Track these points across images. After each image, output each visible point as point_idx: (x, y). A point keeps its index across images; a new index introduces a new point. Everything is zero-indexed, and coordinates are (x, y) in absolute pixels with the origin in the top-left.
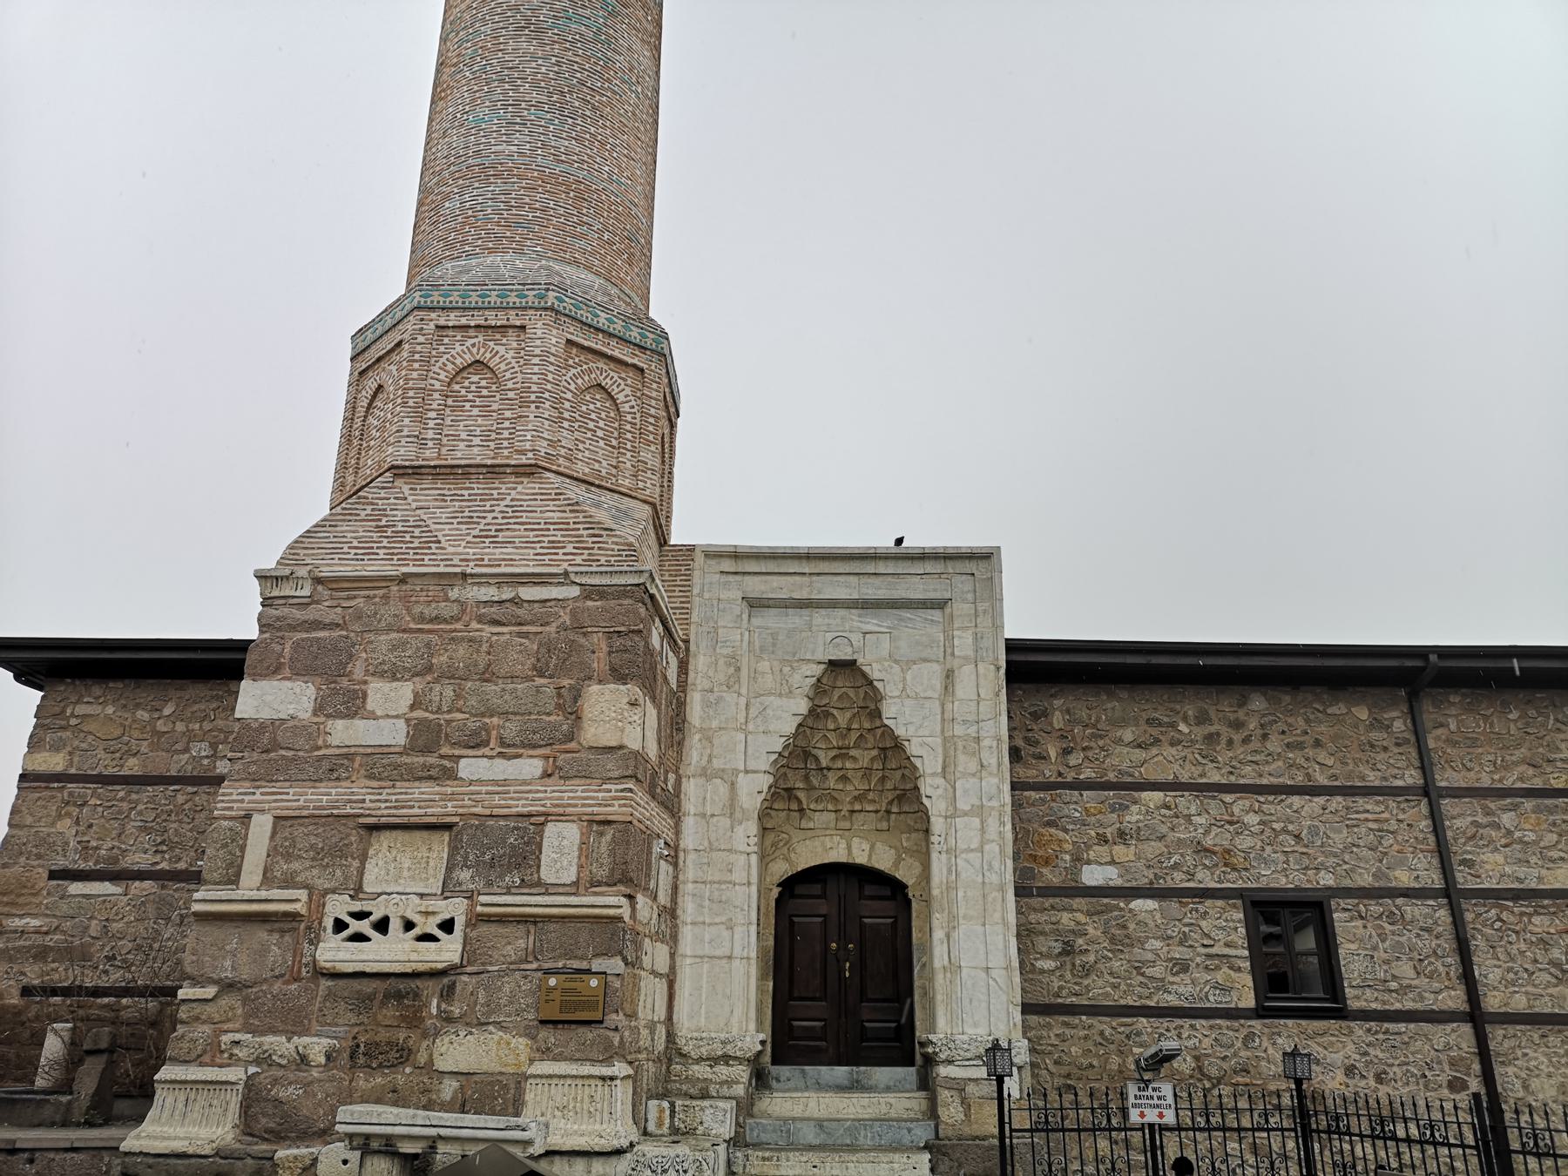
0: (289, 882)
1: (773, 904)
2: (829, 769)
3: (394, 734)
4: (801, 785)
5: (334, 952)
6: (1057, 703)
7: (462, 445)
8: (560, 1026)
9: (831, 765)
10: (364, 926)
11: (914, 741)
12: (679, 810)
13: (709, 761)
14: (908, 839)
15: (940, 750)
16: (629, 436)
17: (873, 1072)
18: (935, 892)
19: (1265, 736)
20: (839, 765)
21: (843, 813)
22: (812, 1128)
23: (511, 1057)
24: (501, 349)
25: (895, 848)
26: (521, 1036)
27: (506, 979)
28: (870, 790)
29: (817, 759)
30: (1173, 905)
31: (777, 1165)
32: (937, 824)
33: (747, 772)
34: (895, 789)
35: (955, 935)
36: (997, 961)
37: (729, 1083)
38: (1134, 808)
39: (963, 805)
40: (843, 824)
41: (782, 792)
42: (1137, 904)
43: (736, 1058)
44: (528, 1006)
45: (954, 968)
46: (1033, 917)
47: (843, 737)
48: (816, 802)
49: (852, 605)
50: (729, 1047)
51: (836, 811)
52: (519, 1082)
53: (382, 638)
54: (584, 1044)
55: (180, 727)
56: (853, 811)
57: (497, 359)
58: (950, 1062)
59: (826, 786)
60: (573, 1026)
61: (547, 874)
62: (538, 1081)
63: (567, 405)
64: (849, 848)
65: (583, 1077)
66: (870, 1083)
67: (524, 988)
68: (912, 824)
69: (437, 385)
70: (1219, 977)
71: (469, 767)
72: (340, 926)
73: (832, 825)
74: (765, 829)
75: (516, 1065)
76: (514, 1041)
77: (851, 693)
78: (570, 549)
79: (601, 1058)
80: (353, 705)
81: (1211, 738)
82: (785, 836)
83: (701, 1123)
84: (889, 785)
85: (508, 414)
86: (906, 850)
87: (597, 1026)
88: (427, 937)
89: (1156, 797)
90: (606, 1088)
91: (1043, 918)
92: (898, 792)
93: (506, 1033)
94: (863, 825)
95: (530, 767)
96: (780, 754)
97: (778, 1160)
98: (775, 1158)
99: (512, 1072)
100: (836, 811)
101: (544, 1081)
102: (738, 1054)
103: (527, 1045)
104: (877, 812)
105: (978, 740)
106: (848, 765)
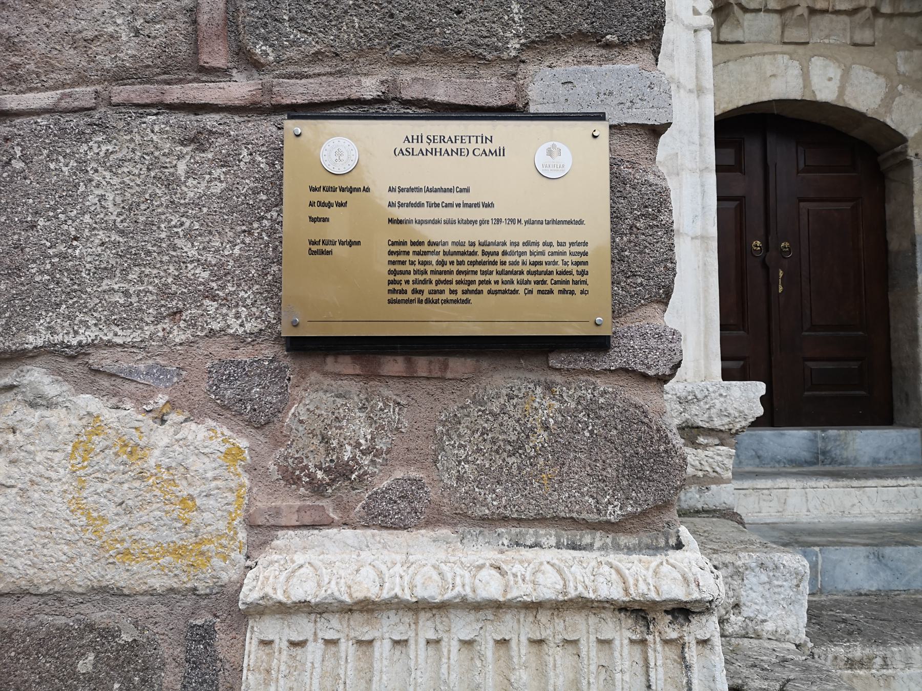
8: (394, 365)
17: (850, 438)
21: (799, 11)
22: (862, 560)
23: (154, 512)
25: (887, 76)
26: (195, 414)
27: (98, 146)
31: (887, 678)
40: (795, 34)
43: (711, 432)
44: (220, 273)
50: (694, 409)
51: (780, 12)
52: (205, 635)
54: (517, 448)
60: (459, 366)
62: (302, 628)
64: (805, 75)
65: (533, 607)
66: (845, 454)
67: (192, 189)
73: (775, 35)
75: (178, 551)
76: (162, 436)
79: (613, 513)
83: (737, 606)
86: (906, 80)
87: (581, 361)
90: (659, 656)
93: (116, 398)
94: (828, 37)
97: (885, 665)
98: (879, 661)
99: (158, 583)
100: (780, 12)
101: (332, 628)
102: (717, 423)
103: (233, 455)
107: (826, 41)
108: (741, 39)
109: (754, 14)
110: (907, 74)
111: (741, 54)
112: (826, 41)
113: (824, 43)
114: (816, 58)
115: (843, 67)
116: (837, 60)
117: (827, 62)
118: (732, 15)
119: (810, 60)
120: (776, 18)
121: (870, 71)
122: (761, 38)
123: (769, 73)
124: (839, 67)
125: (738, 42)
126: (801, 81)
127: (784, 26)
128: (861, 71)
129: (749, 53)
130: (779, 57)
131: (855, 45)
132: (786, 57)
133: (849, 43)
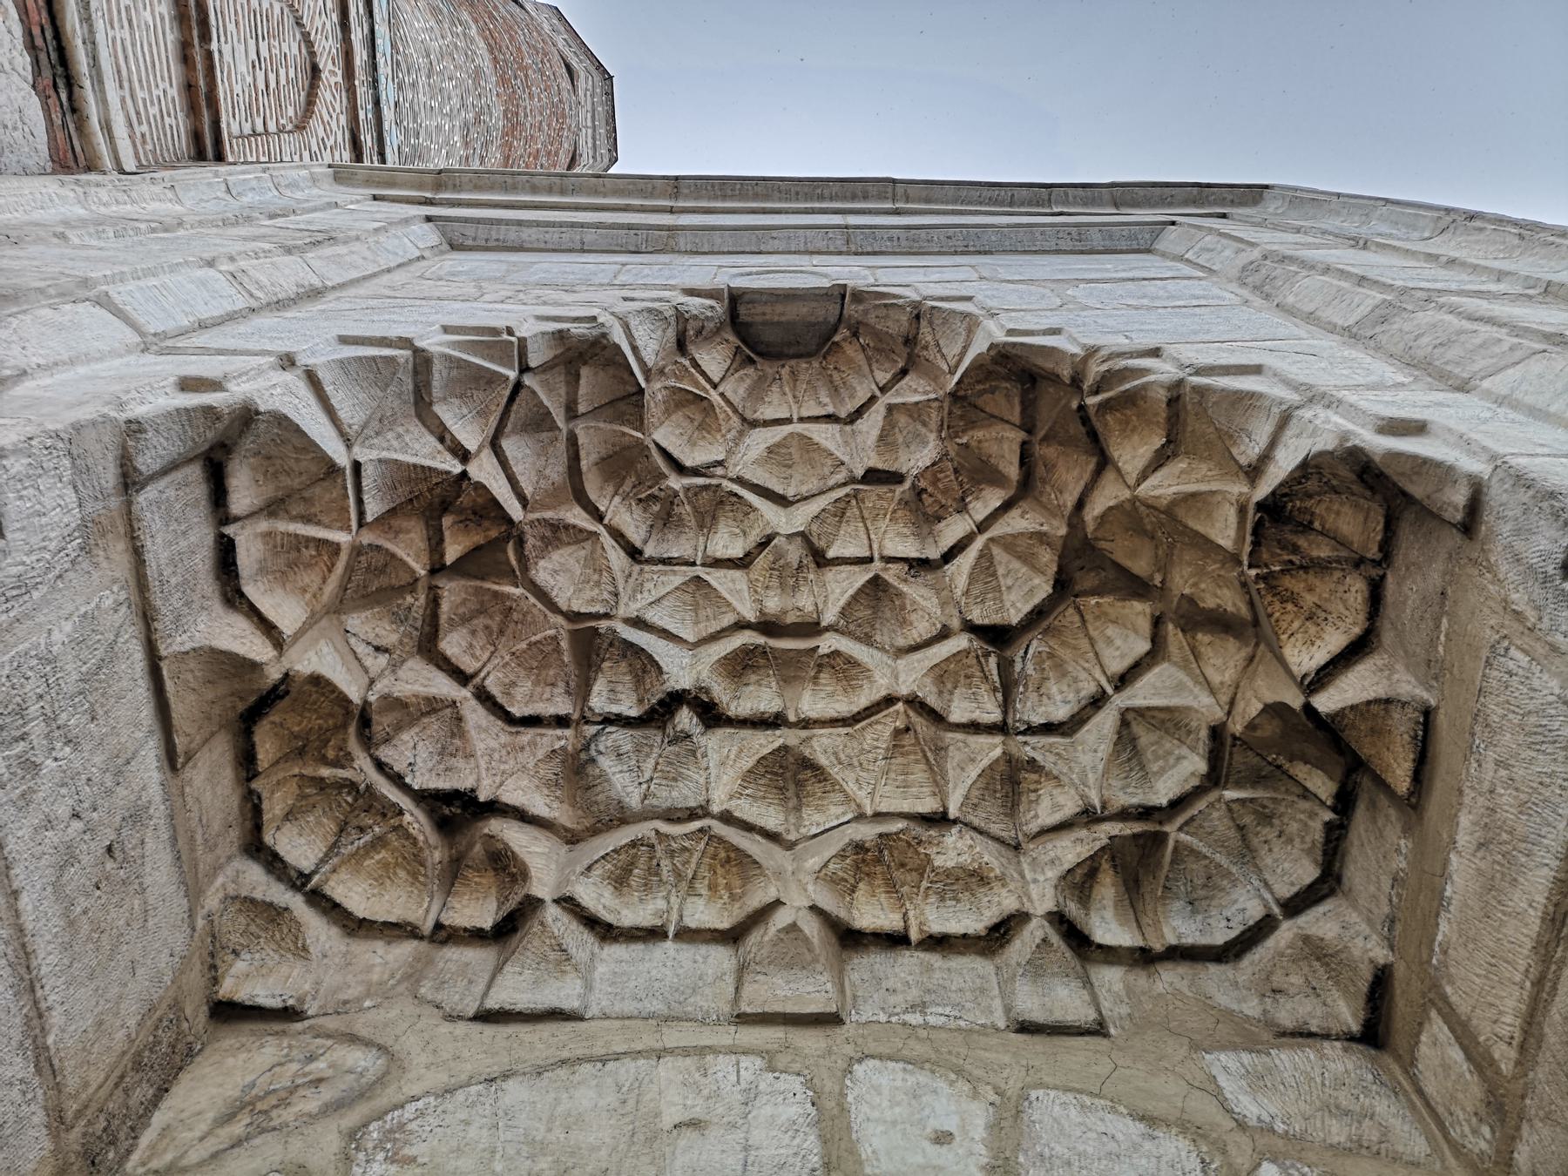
2: (711, 715)
4: (539, 805)
9: (721, 692)
14: (1257, 1081)
20: (760, 697)
21: (781, 919)
25: (1187, 1127)
28: (939, 820)
29: (643, 665)
34: (1089, 816)
41: (416, 820)
47: (789, 578)
48: (620, 881)
49: (821, 245)
51: (732, 936)
56: (849, 938)
59: (684, 795)
68: (1252, 1008)
74: (228, 1012)
77: (824, 434)
82: (360, 1059)
84: (1050, 806)
92: (1115, 828)
96: (422, 362)
100: (732, 936)
104: (1001, 933)
106: (813, 702)
107: (915, 1019)
108: (570, 1003)
109: (638, 948)
110: (1280, 1127)
111: (565, 1054)
112: (915, 1019)
113: (904, 1024)
114: (871, 1063)
115: (993, 1097)
116: (959, 1072)
117: (923, 1077)
118: (536, 928)
119: (848, 1071)
120: (720, 958)
121: (1113, 1110)
122: (657, 1006)
123: (671, 1116)
124: (975, 1095)
125: (555, 1015)
126: (811, 1142)
127: (741, 970)
128: (1073, 1112)
129: (599, 1050)
130: (723, 1064)
131: (1026, 1028)
132: (751, 1064)
133: (1002, 1024)
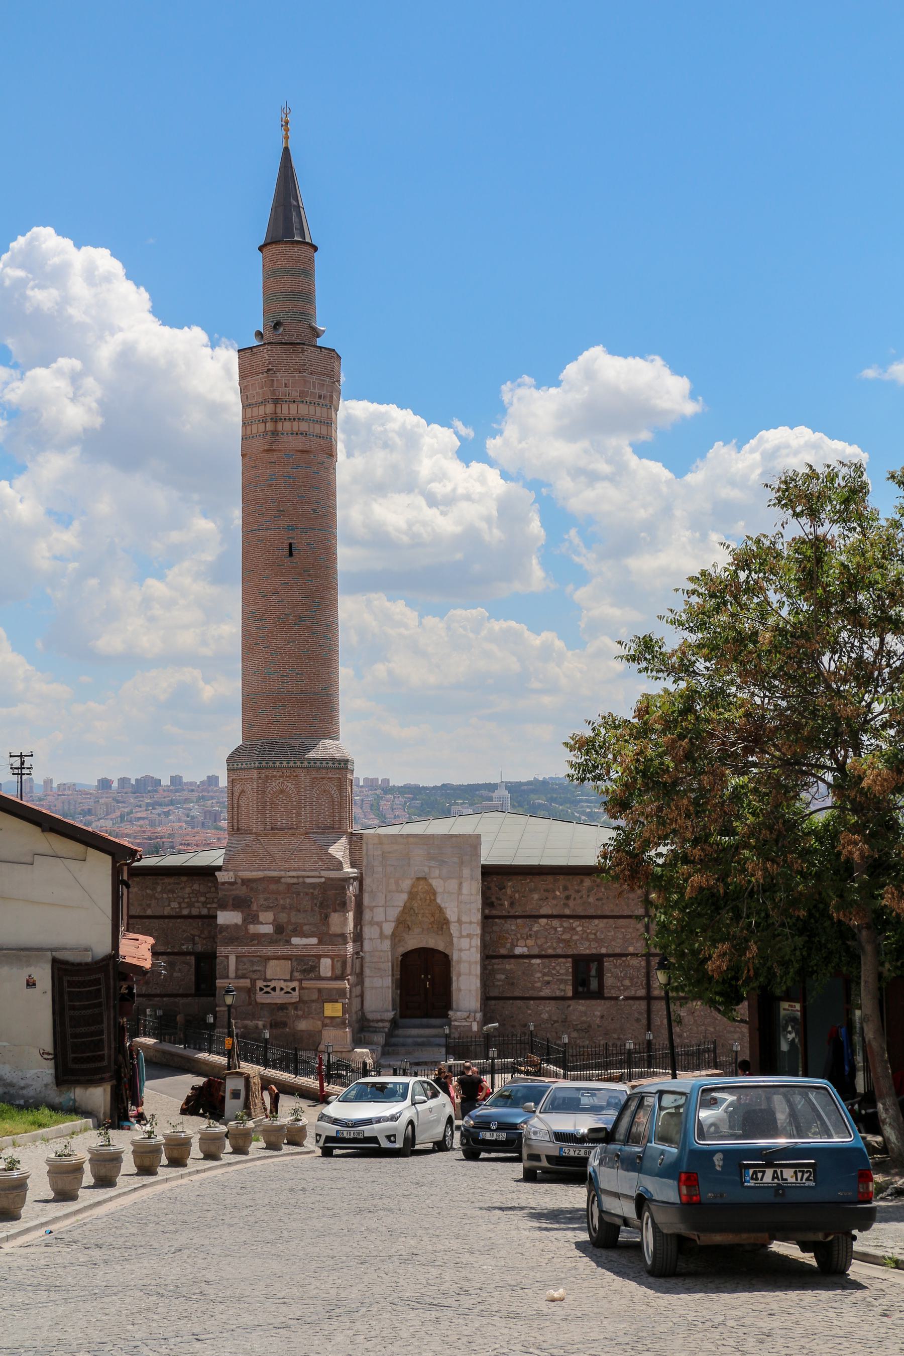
0: (244, 977)
1: (399, 963)
3: (268, 929)
5: (261, 998)
6: (510, 884)
7: (279, 823)
10: (268, 989)
11: (448, 909)
12: (362, 937)
13: (372, 918)
15: (457, 914)
16: (337, 807)
18: (454, 964)
19: (588, 896)
24: (289, 784)
30: (546, 961)
32: (455, 940)
33: (386, 921)
35: (460, 978)
36: (473, 988)
37: (384, 1027)
38: (536, 925)
39: (464, 933)
42: (534, 961)
45: (459, 990)
46: (495, 967)
53: (261, 896)
55: (165, 896)
57: (288, 789)
58: (455, 1020)
61: (322, 974)
63: (314, 803)
69: (268, 800)
70: (562, 987)
71: (295, 940)
72: (261, 989)
78: (320, 864)
80: (255, 919)
81: (568, 898)
85: (294, 811)
88: (287, 993)
89: (543, 921)
91: (499, 967)
95: (314, 941)
105: (470, 910)
